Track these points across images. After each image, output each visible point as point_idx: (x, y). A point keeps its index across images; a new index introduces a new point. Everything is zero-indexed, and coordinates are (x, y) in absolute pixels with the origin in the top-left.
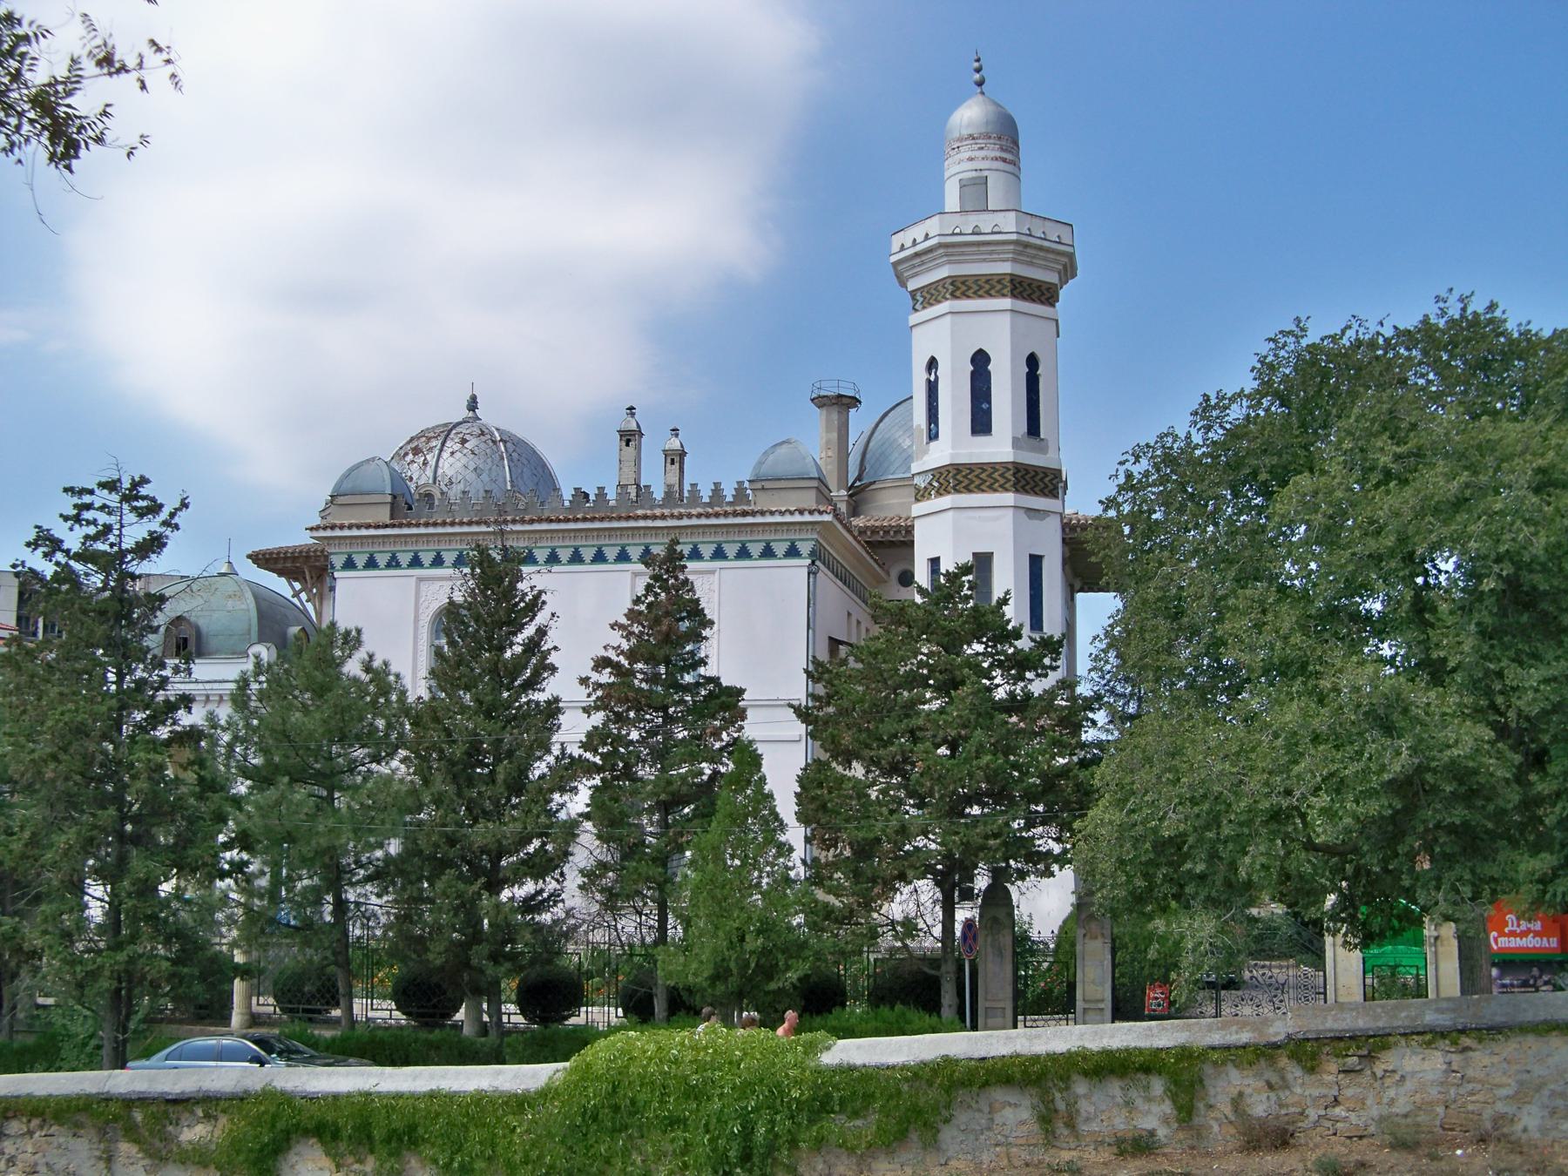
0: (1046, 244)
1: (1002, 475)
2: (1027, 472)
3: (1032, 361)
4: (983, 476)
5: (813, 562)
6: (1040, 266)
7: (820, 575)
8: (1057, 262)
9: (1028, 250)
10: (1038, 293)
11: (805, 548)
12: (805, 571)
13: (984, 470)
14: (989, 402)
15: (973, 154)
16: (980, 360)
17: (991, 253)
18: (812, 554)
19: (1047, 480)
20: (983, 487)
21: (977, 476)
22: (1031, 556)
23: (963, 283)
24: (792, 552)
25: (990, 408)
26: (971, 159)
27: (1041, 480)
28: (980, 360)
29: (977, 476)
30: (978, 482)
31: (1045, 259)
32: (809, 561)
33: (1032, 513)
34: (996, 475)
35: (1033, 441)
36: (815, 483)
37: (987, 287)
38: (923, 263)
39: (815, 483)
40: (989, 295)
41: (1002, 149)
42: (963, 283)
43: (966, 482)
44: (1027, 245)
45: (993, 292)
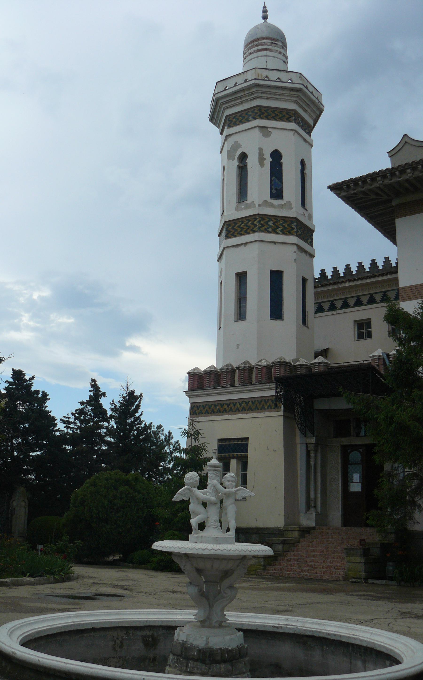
1: (252, 224)
20: (242, 232)
22: (272, 272)
29: (239, 227)
40: (248, 121)
43: (233, 231)
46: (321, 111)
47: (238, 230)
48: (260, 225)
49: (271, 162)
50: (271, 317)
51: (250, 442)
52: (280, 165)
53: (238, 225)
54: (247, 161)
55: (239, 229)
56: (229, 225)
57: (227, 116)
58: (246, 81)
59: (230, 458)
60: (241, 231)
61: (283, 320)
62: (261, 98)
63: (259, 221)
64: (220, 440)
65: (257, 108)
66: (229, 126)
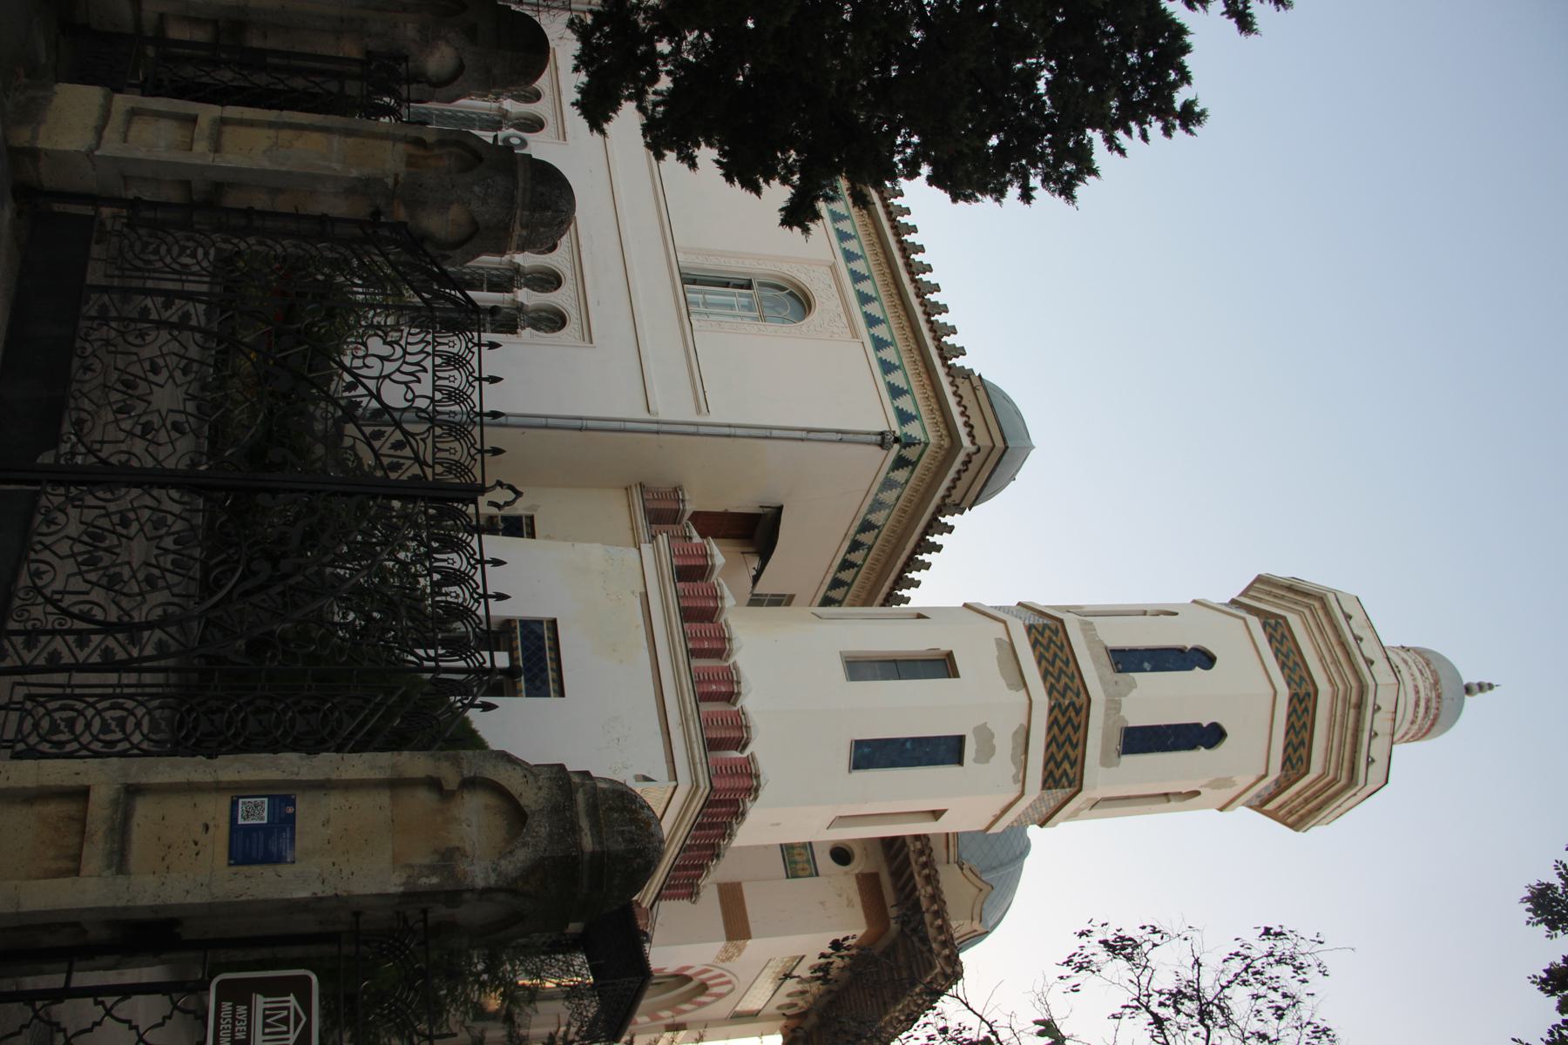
0: (1366, 736)
1: (1066, 687)
2: (1076, 729)
3: (1212, 736)
4: (1058, 663)
5: (897, 440)
6: (1330, 740)
7: (881, 453)
8: (1339, 766)
9: (1352, 711)
10: (1295, 741)
11: (913, 430)
12: (884, 427)
13: (1067, 663)
14: (1153, 670)
15: (1410, 662)
16: (1205, 659)
17: (1336, 662)
18: (908, 443)
19: (1066, 765)
20: (1044, 663)
21: (1055, 655)
23: (1283, 636)
24: (904, 417)
25: (1145, 671)
26: (1405, 662)
27: (1066, 756)
28: (1205, 659)
30: (1049, 656)
31: (1341, 745)
32: (898, 433)
33: (1021, 740)
34: (1064, 679)
35: (1116, 741)
36: (999, 444)
37: (1291, 664)
38: (1282, 598)
39: (999, 444)
40: (1283, 666)
41: (1428, 701)
42: (1283, 636)
43: (1045, 642)
44: (1360, 706)
45: (1286, 671)
46: (1294, 826)
47: (1048, 651)
48: (1064, 707)
49: (1198, 725)
50: (857, 742)
51: (553, 701)
52: (1192, 746)
53: (1059, 653)
54: (1197, 668)
55: (1049, 656)
56: (1056, 632)
57: (1284, 618)
58: (1370, 662)
59: (512, 652)
60: (1047, 660)
61: (850, 771)
62: (1335, 695)
63: (1072, 704)
64: (554, 622)
65: (1311, 689)
66: (1264, 626)
